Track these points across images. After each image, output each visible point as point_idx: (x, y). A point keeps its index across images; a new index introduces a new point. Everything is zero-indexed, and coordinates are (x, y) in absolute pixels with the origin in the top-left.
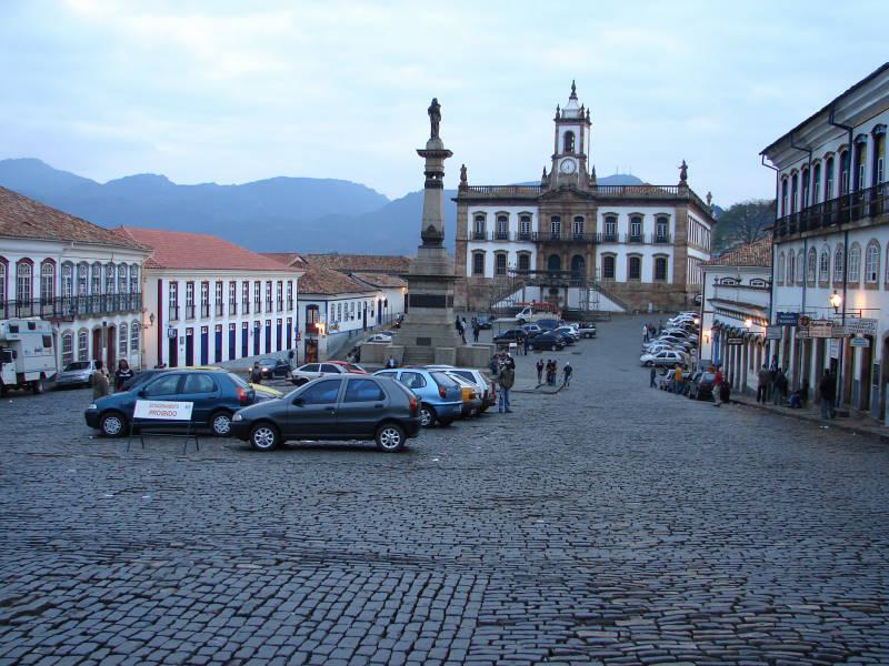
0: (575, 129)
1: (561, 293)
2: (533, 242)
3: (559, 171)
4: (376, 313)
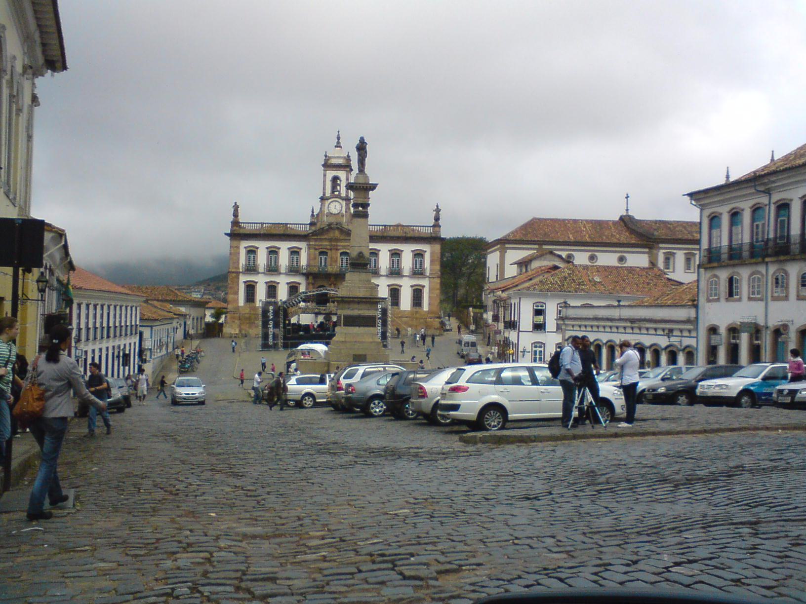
2: (303, 274)
3: (326, 211)
4: (172, 341)
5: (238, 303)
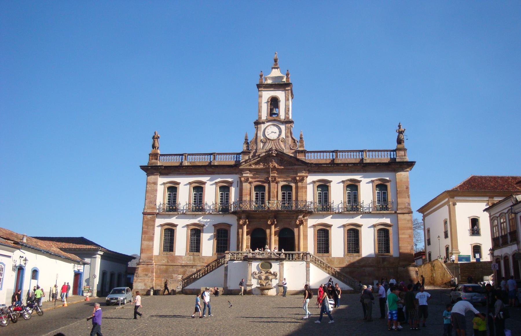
0: (280, 94)
1: (275, 267)
5: (152, 252)
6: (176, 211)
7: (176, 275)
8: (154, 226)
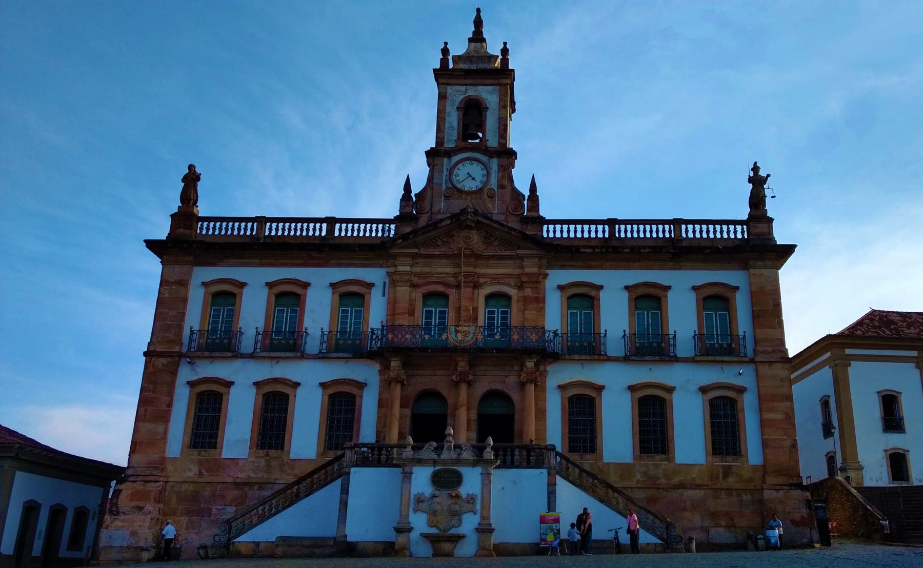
2: (371, 355)
5: (164, 452)
6: (229, 350)
7: (220, 507)
8: (171, 386)
